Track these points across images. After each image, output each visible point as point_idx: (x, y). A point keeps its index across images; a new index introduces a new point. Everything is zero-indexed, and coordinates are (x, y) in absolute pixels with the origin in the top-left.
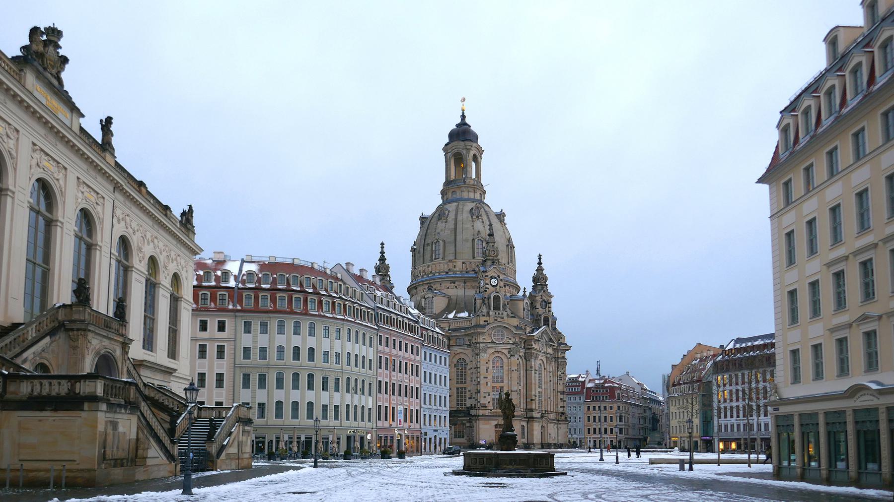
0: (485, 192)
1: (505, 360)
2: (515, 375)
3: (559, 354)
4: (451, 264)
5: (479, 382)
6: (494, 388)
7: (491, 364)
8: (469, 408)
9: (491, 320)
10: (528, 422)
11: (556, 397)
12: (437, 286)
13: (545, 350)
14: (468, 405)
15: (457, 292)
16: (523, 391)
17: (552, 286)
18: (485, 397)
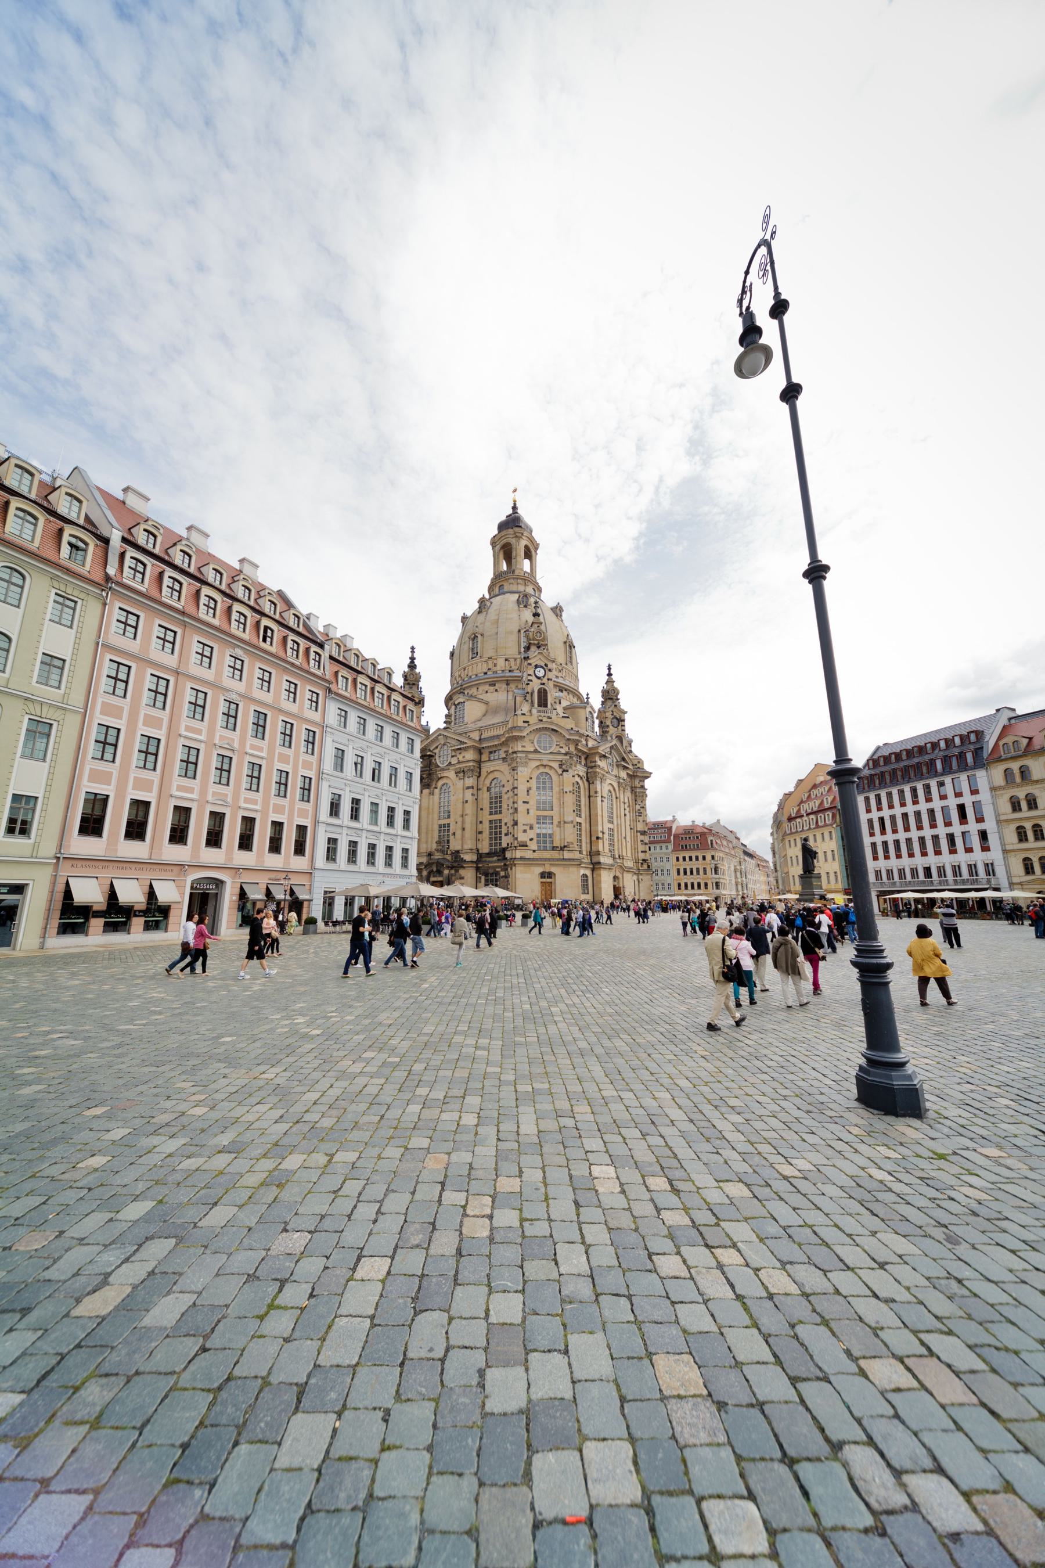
0: (540, 590)
1: (555, 778)
2: (570, 799)
3: (637, 783)
4: (490, 662)
5: (516, 809)
6: (538, 817)
7: (533, 783)
8: (504, 850)
9: (533, 720)
10: (593, 870)
11: (634, 840)
12: (473, 691)
13: (615, 772)
14: (504, 845)
15: (499, 697)
16: (585, 827)
17: (625, 702)
18: (525, 831)
